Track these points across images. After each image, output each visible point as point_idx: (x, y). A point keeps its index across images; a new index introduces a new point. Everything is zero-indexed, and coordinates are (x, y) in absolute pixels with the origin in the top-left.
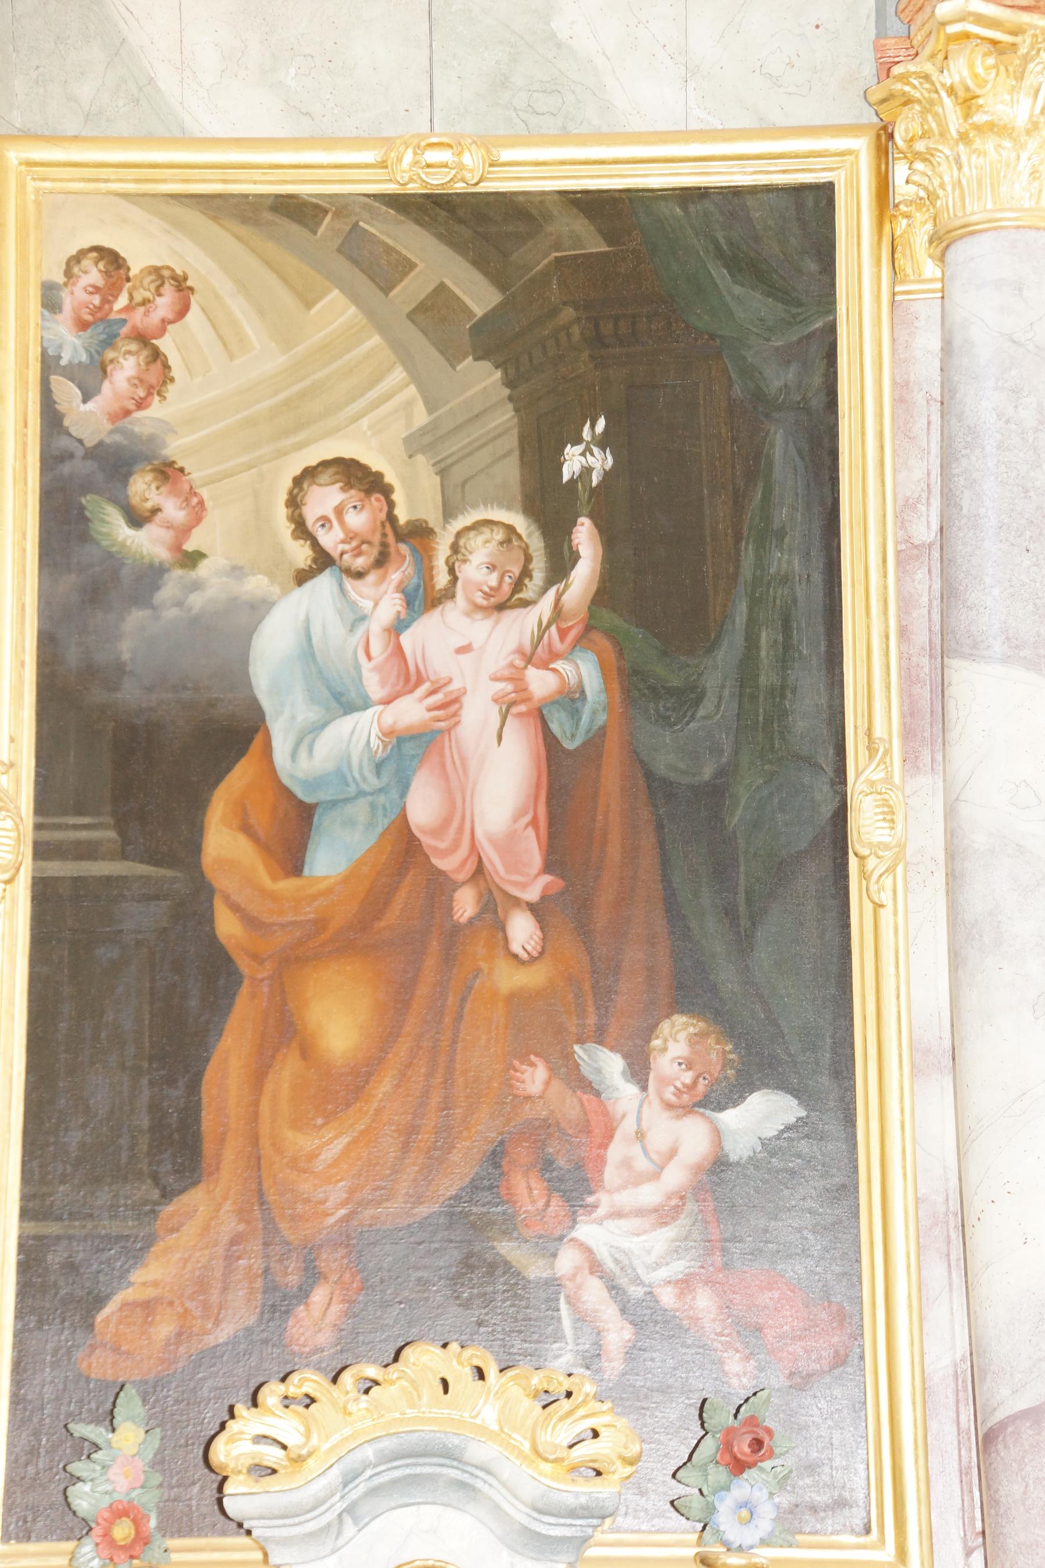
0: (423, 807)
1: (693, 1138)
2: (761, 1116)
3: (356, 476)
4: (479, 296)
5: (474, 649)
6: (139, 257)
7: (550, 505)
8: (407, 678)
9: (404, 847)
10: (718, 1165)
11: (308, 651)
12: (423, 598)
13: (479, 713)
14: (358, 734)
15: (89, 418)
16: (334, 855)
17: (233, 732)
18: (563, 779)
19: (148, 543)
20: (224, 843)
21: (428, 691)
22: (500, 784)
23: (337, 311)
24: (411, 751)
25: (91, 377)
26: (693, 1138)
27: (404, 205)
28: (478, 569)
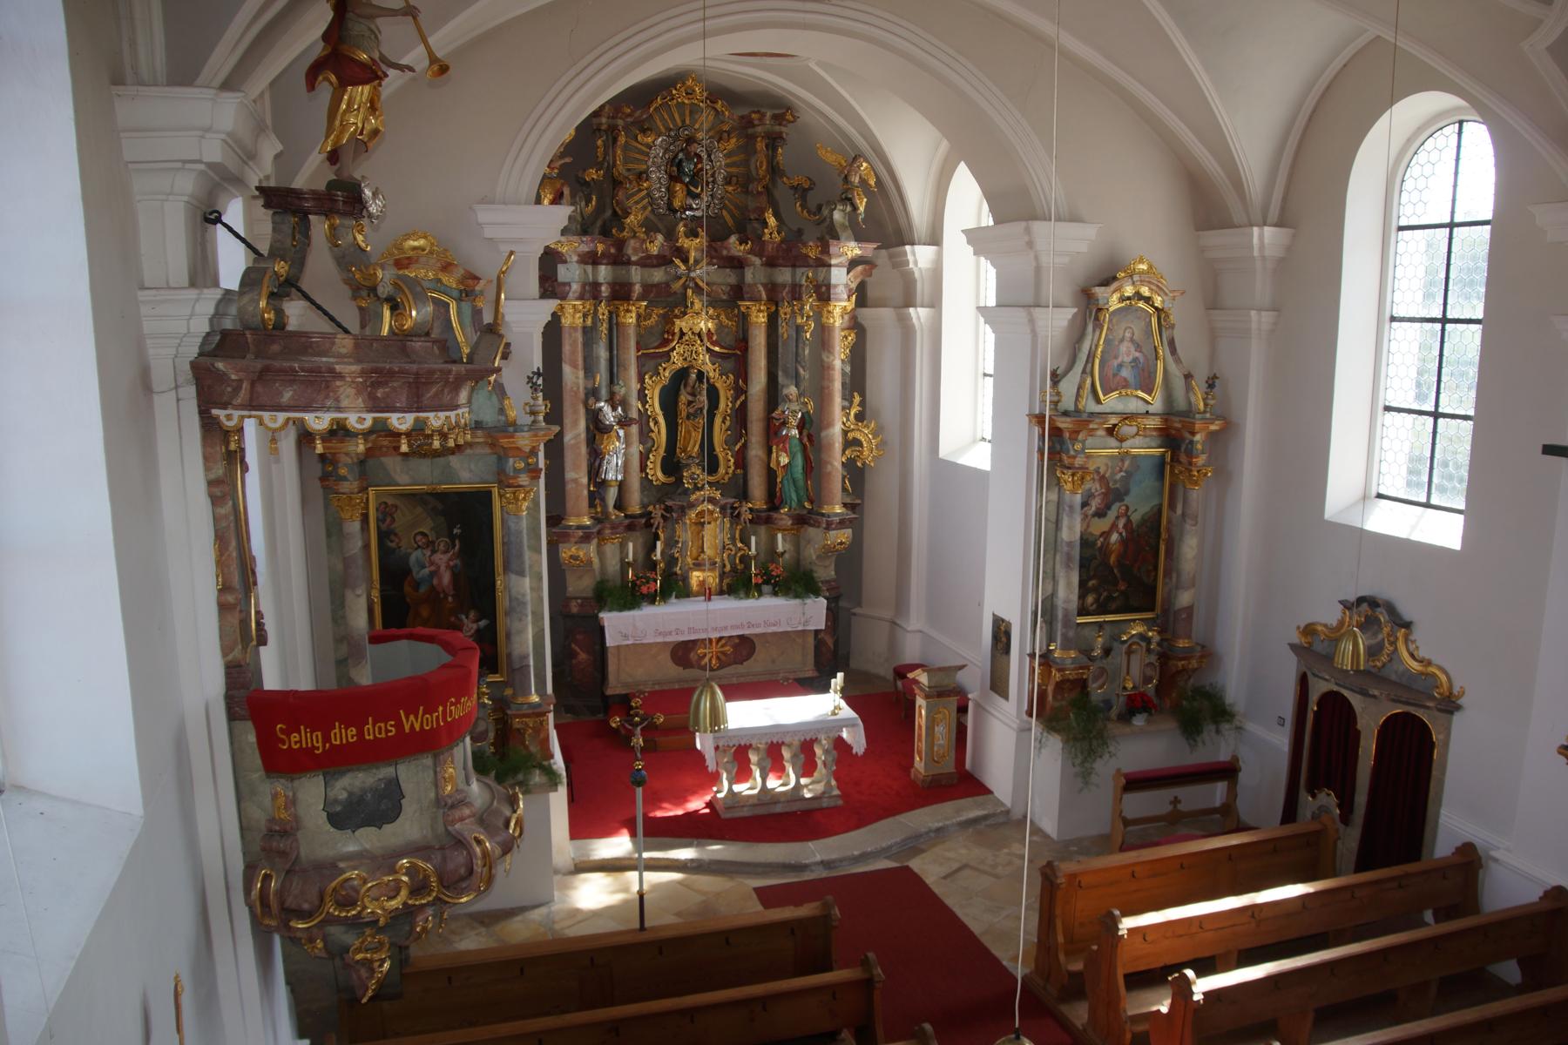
0: (435, 582)
1: (475, 626)
2: (483, 623)
3: (422, 534)
4: (440, 507)
5: (441, 559)
6: (390, 501)
7: (452, 538)
8: (432, 563)
9: (433, 588)
10: (478, 630)
11: (417, 560)
12: (434, 552)
13: (443, 568)
14: (426, 571)
15: (384, 527)
16: (423, 589)
17: (408, 572)
18: (455, 577)
19: (393, 545)
20: (407, 589)
21: (437, 565)
22: (446, 578)
23: (419, 510)
24: (433, 574)
25: (384, 521)
26: (475, 626)
27: (431, 494)
28: (442, 547)
